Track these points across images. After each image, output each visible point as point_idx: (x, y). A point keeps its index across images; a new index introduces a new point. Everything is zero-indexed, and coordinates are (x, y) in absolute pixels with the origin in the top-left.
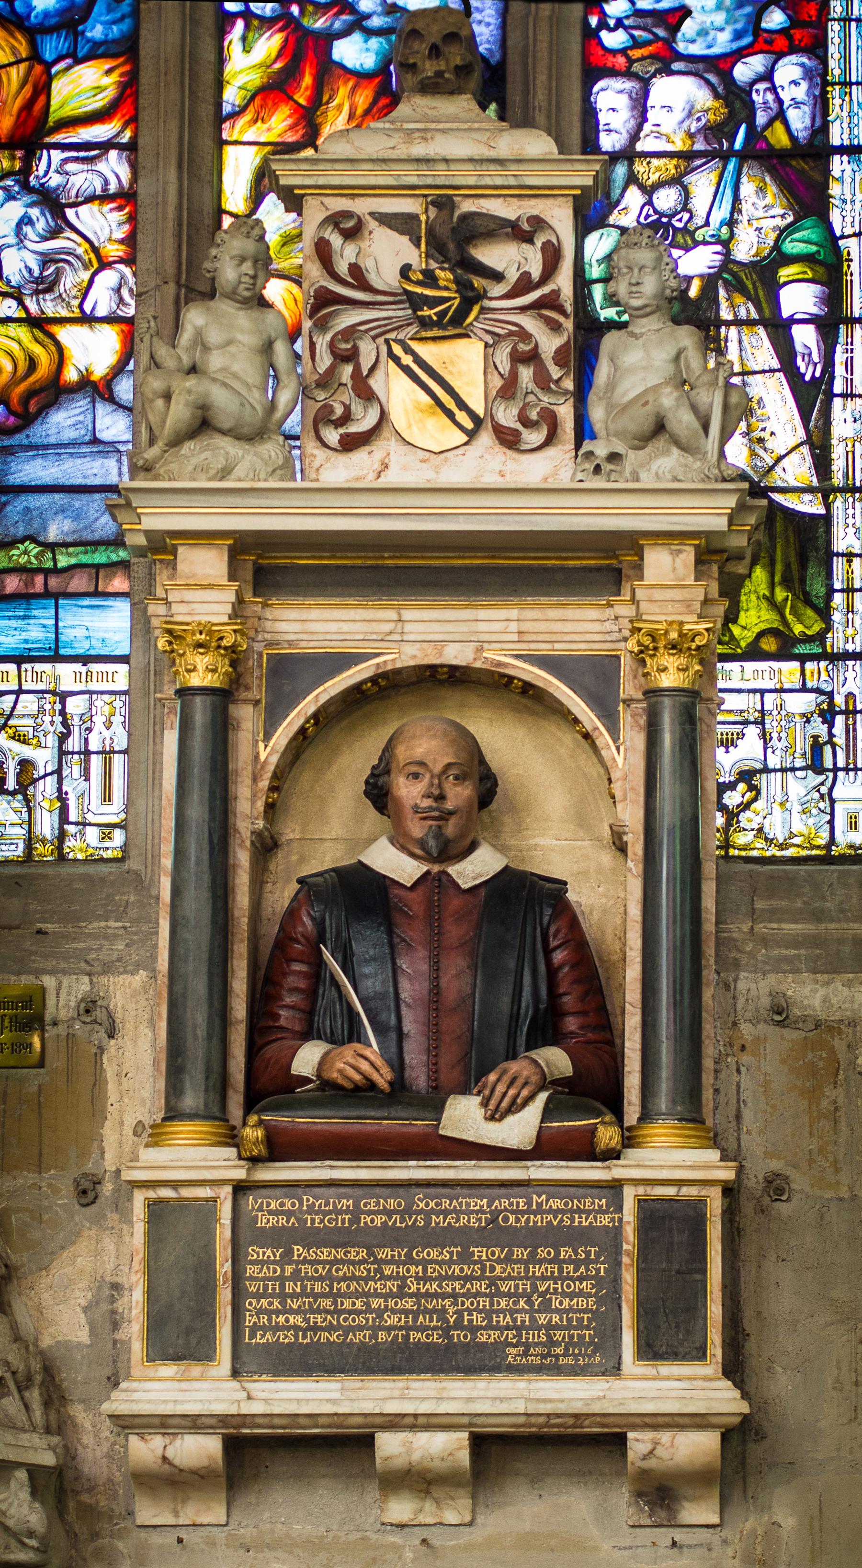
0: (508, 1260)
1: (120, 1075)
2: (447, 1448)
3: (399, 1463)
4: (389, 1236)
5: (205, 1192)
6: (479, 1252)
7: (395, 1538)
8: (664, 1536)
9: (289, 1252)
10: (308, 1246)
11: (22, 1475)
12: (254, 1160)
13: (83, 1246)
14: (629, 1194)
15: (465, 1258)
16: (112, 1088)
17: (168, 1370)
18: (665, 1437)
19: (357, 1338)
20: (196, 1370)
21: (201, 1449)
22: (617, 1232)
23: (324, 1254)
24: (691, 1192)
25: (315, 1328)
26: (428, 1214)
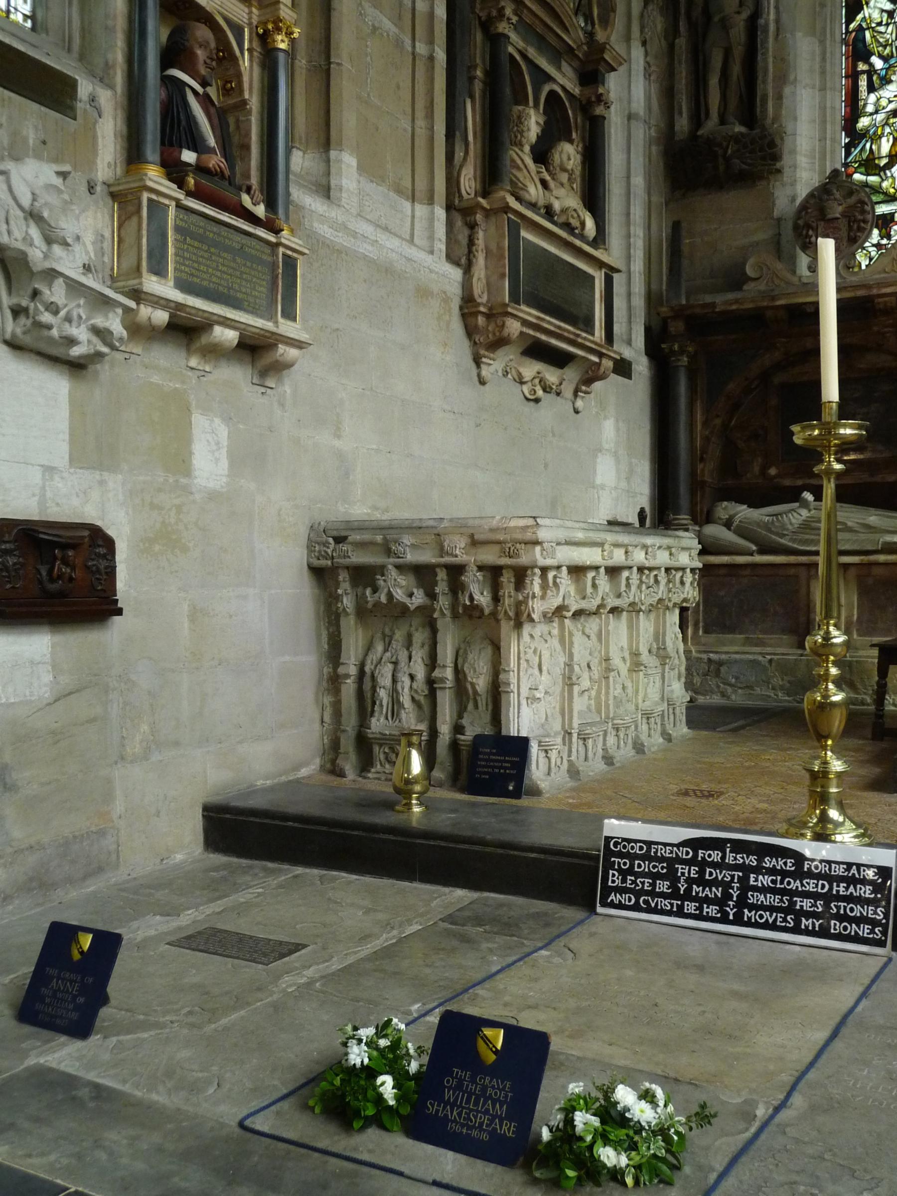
0: (245, 265)
1: (103, 137)
2: (228, 336)
3: (217, 340)
4: (216, 244)
5: (166, 202)
6: (239, 260)
7: (190, 373)
8: (263, 390)
9: (185, 239)
10: (191, 238)
11: (120, 311)
12: (189, 194)
13: (90, 213)
14: (281, 250)
15: (234, 261)
16: (100, 140)
17: (154, 278)
18: (287, 349)
19: (205, 283)
20: (163, 281)
21: (161, 317)
22: (274, 265)
23: (196, 244)
24: (295, 255)
25: (192, 275)
26: (225, 238)
